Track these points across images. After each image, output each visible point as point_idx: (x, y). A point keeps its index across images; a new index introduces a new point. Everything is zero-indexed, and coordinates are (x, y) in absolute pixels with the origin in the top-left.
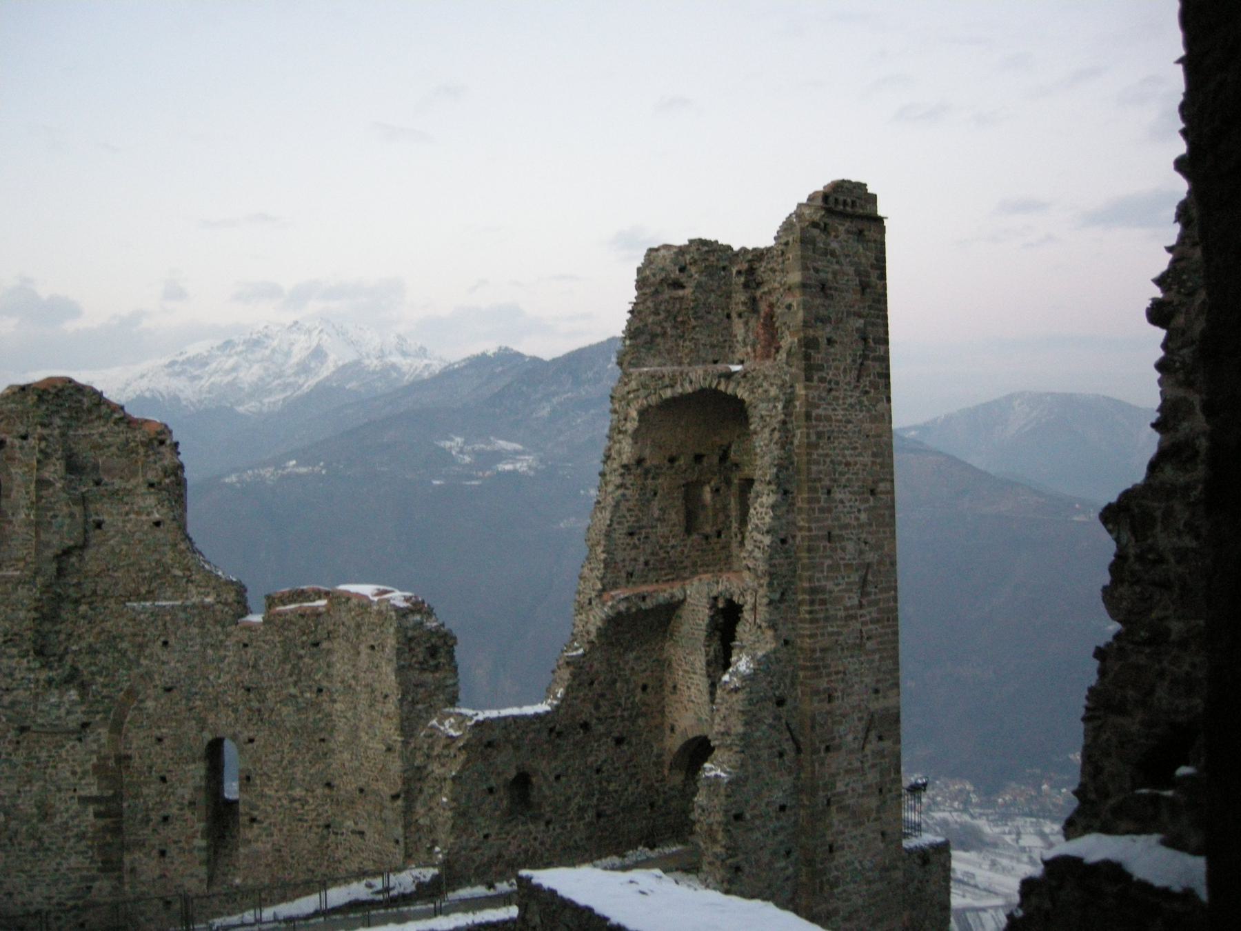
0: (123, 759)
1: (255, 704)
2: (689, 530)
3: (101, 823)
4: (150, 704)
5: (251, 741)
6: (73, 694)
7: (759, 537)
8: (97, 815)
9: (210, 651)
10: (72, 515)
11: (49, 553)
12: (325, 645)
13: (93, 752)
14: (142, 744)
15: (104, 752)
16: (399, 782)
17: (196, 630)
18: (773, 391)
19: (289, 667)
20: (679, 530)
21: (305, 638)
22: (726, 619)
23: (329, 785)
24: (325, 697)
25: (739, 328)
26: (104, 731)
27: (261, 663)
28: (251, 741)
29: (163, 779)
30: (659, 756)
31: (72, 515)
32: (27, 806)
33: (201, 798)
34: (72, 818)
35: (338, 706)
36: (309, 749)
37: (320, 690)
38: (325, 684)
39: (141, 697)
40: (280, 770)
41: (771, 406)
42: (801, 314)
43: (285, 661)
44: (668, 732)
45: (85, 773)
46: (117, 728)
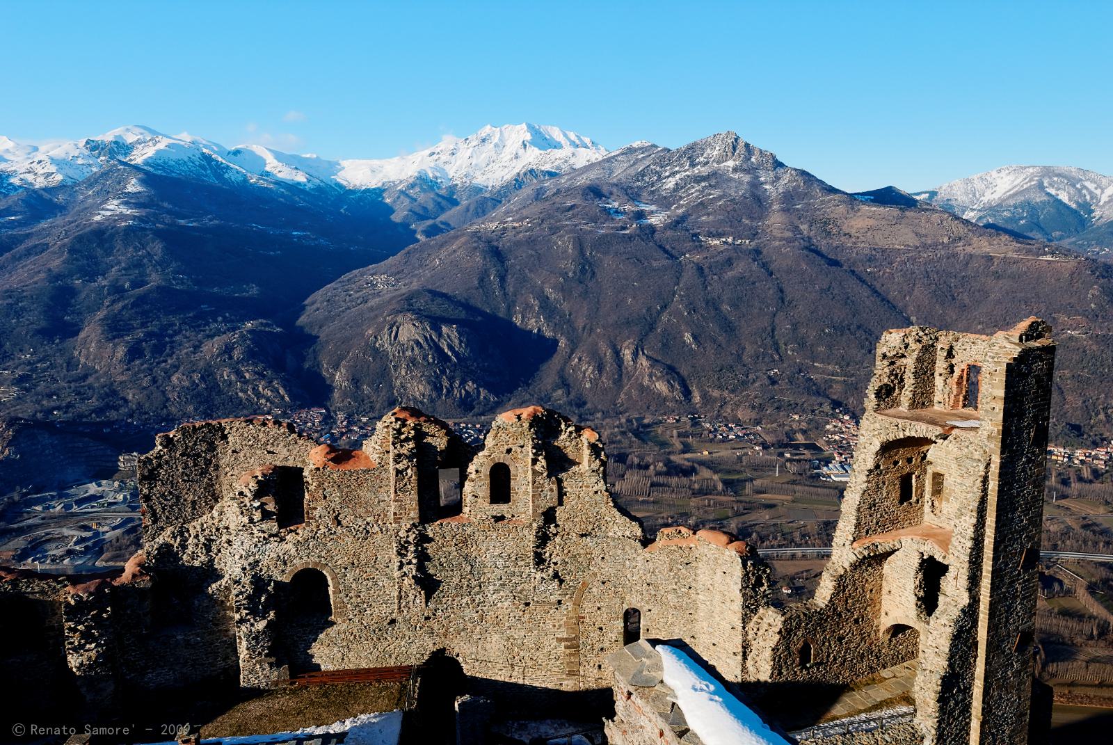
0: (580, 619)
1: (653, 593)
2: (901, 502)
3: (568, 651)
4: (594, 590)
5: (650, 610)
6: (556, 584)
7: (963, 540)
8: (567, 647)
9: (627, 562)
10: (551, 490)
11: (540, 511)
12: (694, 564)
13: (565, 615)
14: (590, 610)
15: (570, 615)
16: (740, 647)
17: (620, 551)
18: (977, 455)
19: (672, 574)
20: (896, 502)
21: (682, 560)
22: (932, 572)
23: (693, 637)
24: (692, 591)
25: (939, 381)
26: (570, 605)
27: (657, 571)
28: (650, 610)
29: (601, 629)
30: (877, 626)
31: (551, 490)
32: (529, 643)
33: (621, 639)
34: (553, 649)
35: (700, 596)
36: (683, 618)
37: (690, 588)
38: (693, 584)
39: (590, 586)
40: (666, 627)
41: (975, 464)
42: (1001, 415)
43: (671, 570)
44: (883, 614)
45: (560, 626)
46: (578, 605)
